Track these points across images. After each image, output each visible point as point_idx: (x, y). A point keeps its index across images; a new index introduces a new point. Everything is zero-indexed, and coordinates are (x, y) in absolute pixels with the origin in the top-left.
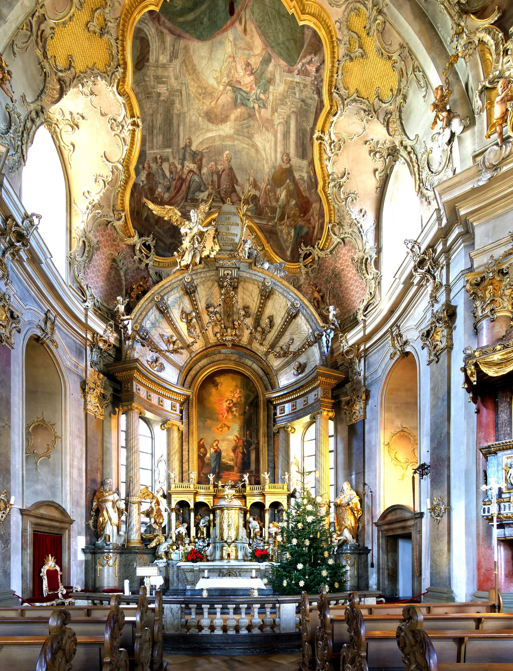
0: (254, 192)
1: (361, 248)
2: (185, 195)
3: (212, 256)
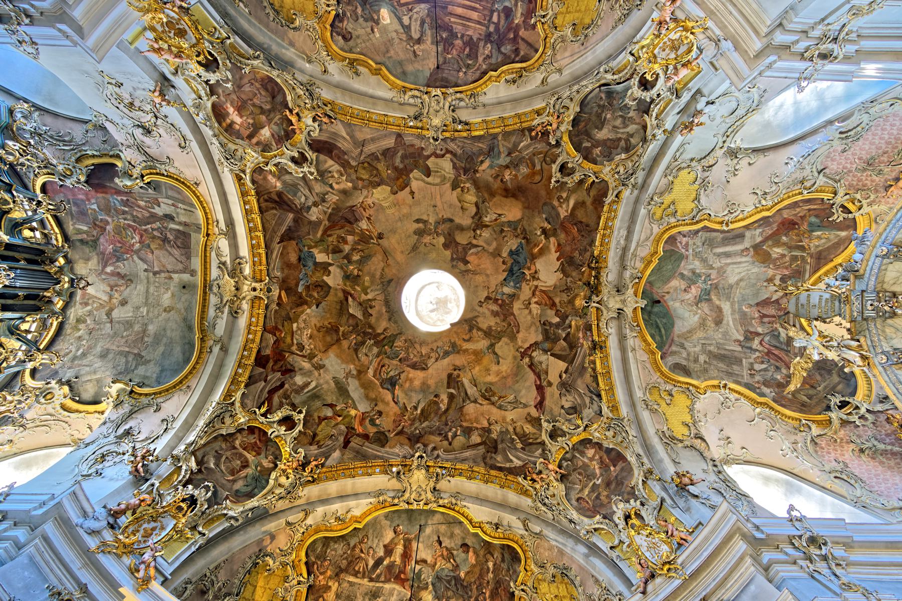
0: (777, 282)
1: (828, 146)
2: (781, 352)
3: (848, 325)
